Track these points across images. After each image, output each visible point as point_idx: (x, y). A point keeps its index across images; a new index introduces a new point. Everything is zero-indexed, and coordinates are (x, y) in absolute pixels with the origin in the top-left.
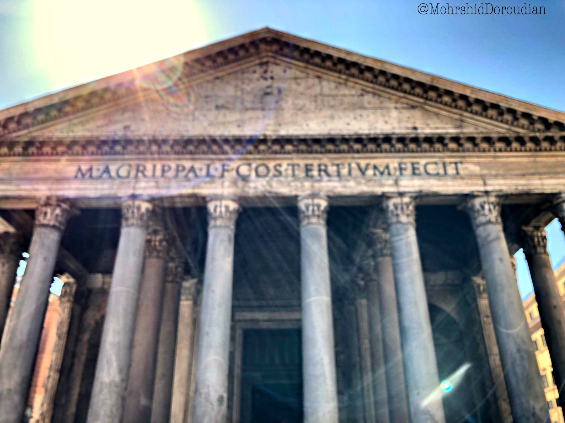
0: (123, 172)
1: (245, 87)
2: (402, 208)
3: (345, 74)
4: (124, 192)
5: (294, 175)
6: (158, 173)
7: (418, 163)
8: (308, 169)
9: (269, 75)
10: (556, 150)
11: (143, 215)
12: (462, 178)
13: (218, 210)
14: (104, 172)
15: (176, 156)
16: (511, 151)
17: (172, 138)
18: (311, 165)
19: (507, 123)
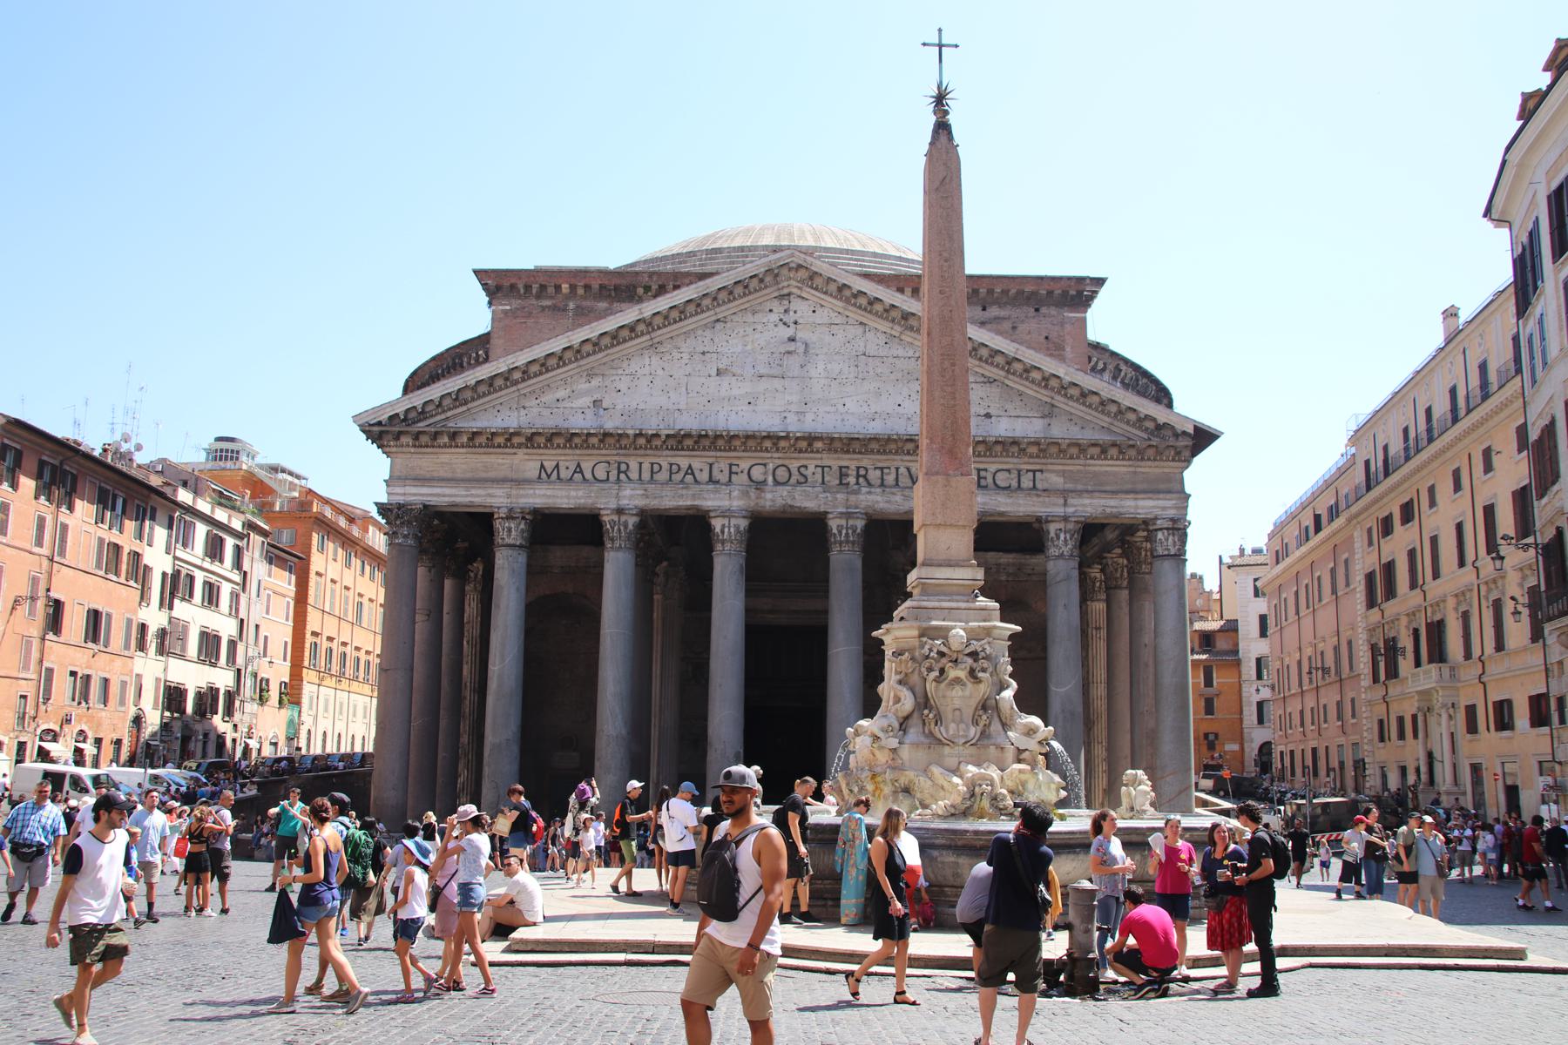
0: (601, 474)
1: (756, 336)
3: (899, 324)
5: (823, 483)
6: (646, 475)
7: (986, 470)
8: (842, 473)
9: (790, 318)
10: (1161, 460)
11: (630, 533)
12: (1038, 496)
13: (726, 530)
14: (575, 472)
16: (1106, 459)
18: (848, 467)
19: (1108, 414)
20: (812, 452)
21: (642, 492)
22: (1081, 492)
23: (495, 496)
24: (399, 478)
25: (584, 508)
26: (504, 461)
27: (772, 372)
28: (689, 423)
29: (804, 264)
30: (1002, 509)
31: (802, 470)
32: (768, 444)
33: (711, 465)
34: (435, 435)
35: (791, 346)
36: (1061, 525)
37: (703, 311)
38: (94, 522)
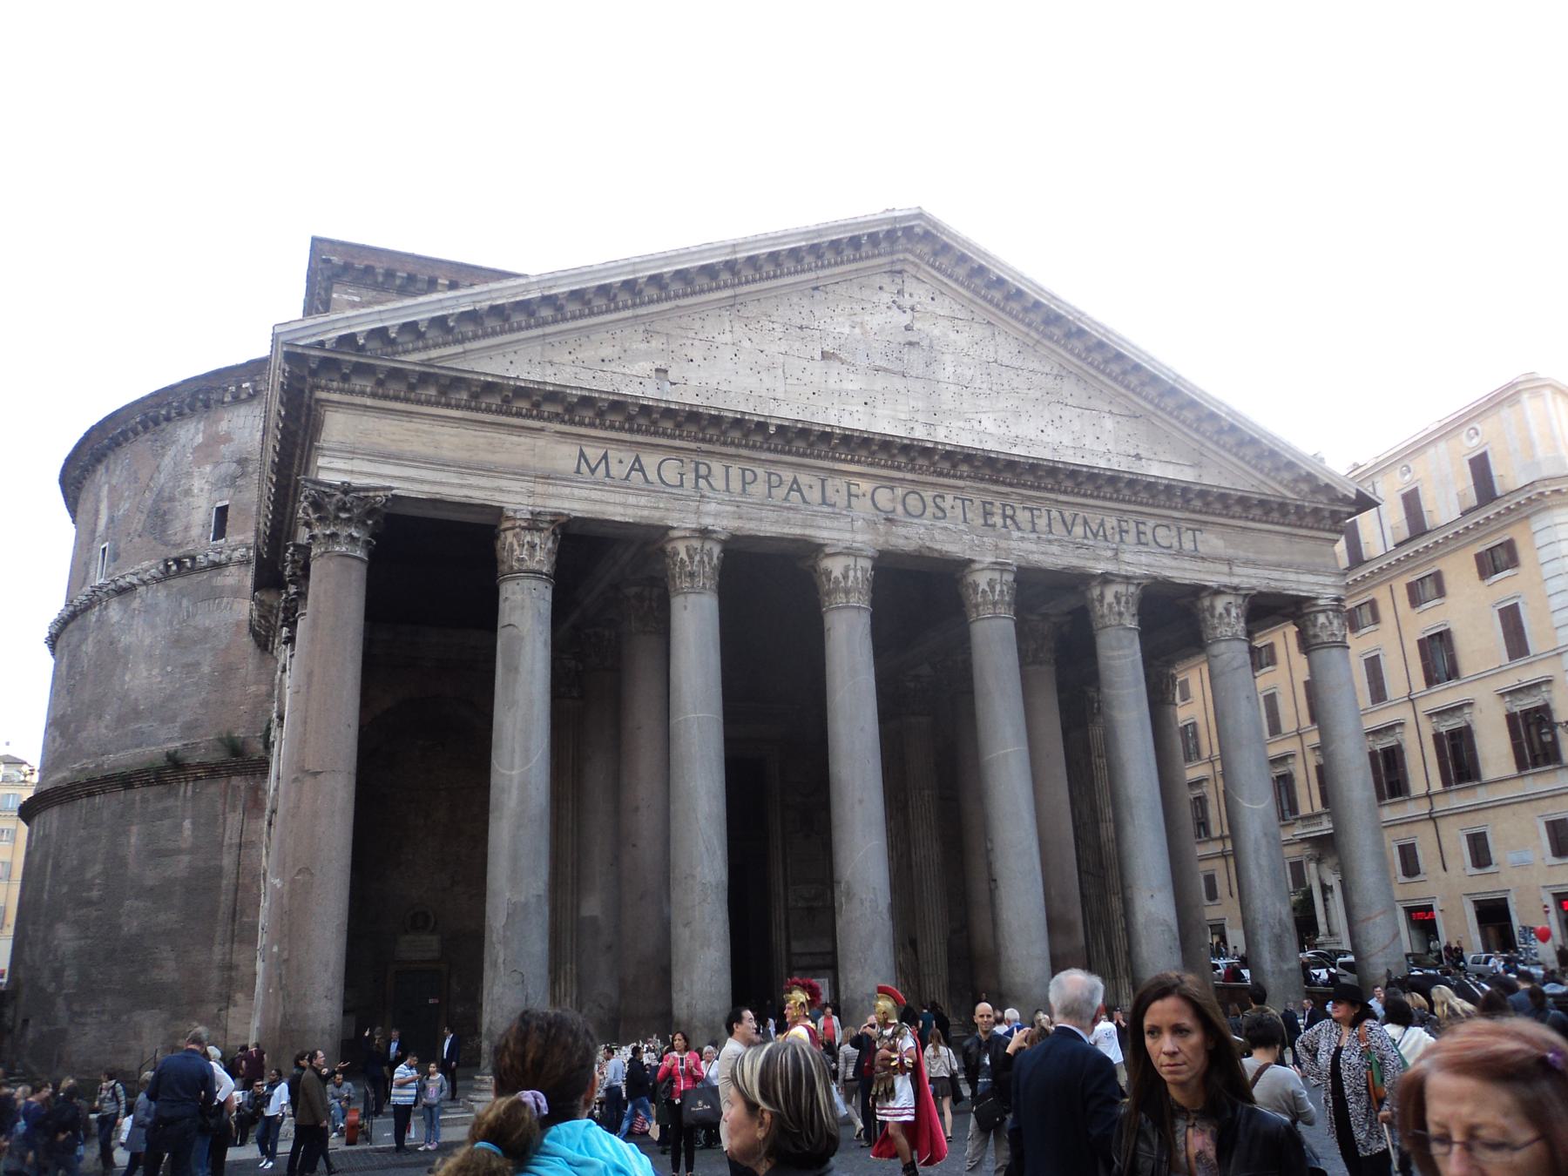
1: (867, 318)
2: (1127, 602)
3: (1037, 330)
4: (681, 519)
5: (965, 520)
6: (736, 485)
9: (906, 301)
10: (1318, 529)
13: (851, 573)
14: (632, 469)
16: (1266, 522)
18: (991, 503)
19: (1261, 471)
20: (954, 476)
23: (509, 492)
26: (522, 439)
27: (890, 366)
29: (934, 232)
30: (1167, 573)
31: (938, 500)
32: (902, 460)
33: (823, 481)
37: (803, 271)
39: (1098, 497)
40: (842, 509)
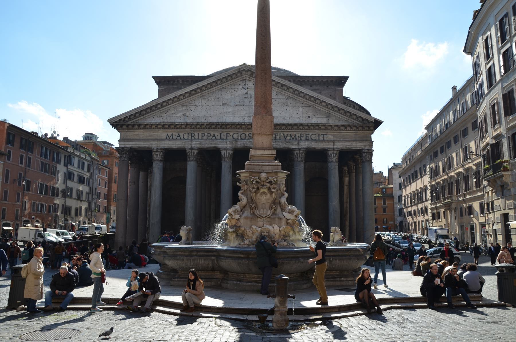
0: (186, 137)
1: (235, 93)
2: (299, 155)
3: (280, 88)
4: (187, 146)
6: (200, 137)
7: (308, 134)
9: (246, 87)
10: (364, 131)
11: (195, 156)
12: (325, 142)
13: (226, 154)
14: (178, 136)
15: (207, 130)
16: (347, 130)
17: (205, 123)
19: (347, 116)
21: (199, 143)
22: (339, 141)
24: (122, 139)
25: (181, 148)
28: (214, 120)
31: (250, 135)
32: (238, 127)
33: (221, 134)
34: (133, 126)
35: (246, 96)
36: (331, 152)
37: (218, 85)
38: (40, 157)
39: (293, 129)
40: (225, 140)
